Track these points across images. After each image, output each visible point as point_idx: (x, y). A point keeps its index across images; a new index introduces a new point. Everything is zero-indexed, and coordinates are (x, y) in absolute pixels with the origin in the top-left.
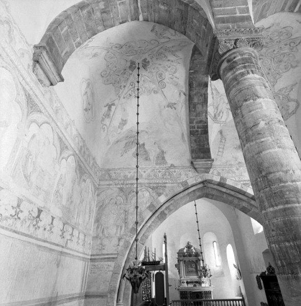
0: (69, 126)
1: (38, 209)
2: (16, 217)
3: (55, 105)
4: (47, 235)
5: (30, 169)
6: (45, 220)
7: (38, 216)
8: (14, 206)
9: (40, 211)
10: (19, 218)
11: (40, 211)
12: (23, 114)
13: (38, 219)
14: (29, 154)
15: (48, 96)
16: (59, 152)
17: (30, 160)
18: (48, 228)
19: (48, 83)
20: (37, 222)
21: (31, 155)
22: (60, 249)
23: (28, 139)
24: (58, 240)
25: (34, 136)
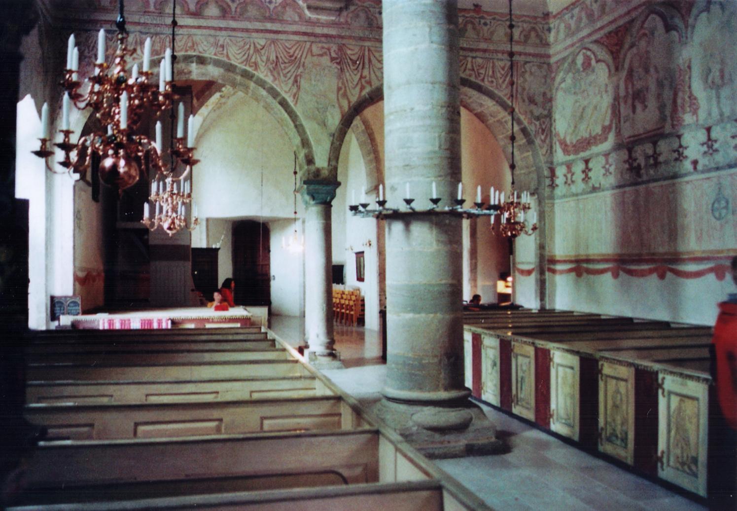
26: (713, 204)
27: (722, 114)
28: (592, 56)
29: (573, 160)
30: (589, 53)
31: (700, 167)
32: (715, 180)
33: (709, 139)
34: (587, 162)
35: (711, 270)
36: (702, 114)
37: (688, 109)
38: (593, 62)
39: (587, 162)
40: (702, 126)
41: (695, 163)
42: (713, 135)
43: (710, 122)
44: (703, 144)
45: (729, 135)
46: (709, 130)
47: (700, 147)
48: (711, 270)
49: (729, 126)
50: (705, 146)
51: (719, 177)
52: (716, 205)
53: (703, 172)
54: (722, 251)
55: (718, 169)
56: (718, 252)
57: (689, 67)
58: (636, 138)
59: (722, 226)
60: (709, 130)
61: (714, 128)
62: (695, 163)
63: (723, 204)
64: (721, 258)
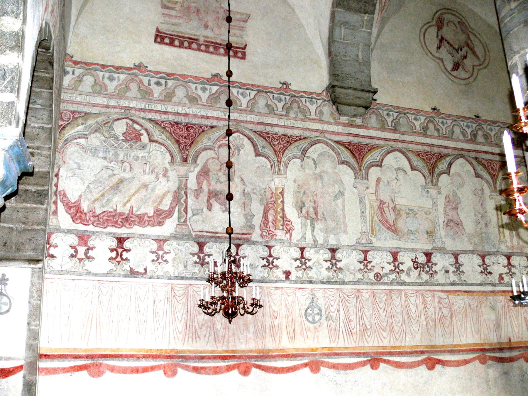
0: (431, 126)
1: (424, 253)
2: (397, 270)
3: (389, 120)
4: (453, 278)
5: (390, 216)
6: (441, 262)
7: (429, 261)
8: (389, 261)
9: (428, 255)
10: (402, 270)
11: (428, 255)
12: (353, 169)
13: (430, 264)
14: (382, 203)
15: (373, 121)
16: (426, 173)
17: (386, 209)
18: (452, 269)
19: (362, 110)
20: (431, 268)
21: (385, 203)
22: (490, 288)
23: (372, 190)
24: (480, 278)
25: (378, 180)
26: (307, 310)
27: (315, 241)
28: (143, 132)
29: (93, 233)
30: (137, 126)
31: (292, 277)
32: (309, 290)
33: (302, 257)
34: (121, 241)
35: (306, 365)
36: (296, 236)
37: (281, 227)
38: (145, 138)
39: (121, 241)
40: (296, 245)
41: (288, 274)
42: (306, 254)
43: (303, 244)
44: (296, 260)
45: (322, 258)
46: (302, 249)
47: (293, 261)
48: (306, 365)
49: (321, 251)
50: (298, 261)
51: (312, 289)
52: (309, 311)
53: (296, 282)
54: (317, 349)
55: (311, 282)
56: (313, 350)
57: (282, 193)
58: (212, 234)
59: (315, 328)
60: (302, 249)
61: (306, 250)
62: (288, 274)
63: (316, 311)
64: (315, 355)
